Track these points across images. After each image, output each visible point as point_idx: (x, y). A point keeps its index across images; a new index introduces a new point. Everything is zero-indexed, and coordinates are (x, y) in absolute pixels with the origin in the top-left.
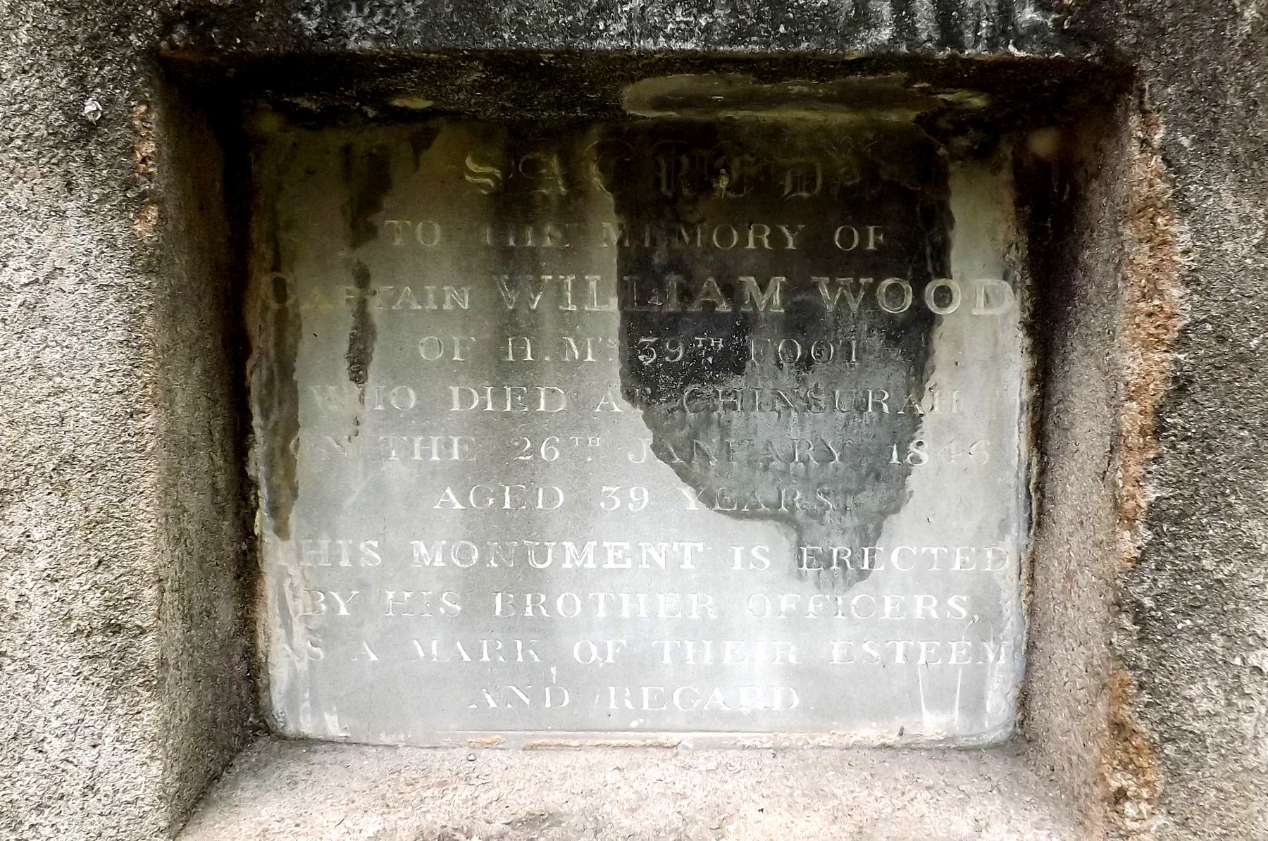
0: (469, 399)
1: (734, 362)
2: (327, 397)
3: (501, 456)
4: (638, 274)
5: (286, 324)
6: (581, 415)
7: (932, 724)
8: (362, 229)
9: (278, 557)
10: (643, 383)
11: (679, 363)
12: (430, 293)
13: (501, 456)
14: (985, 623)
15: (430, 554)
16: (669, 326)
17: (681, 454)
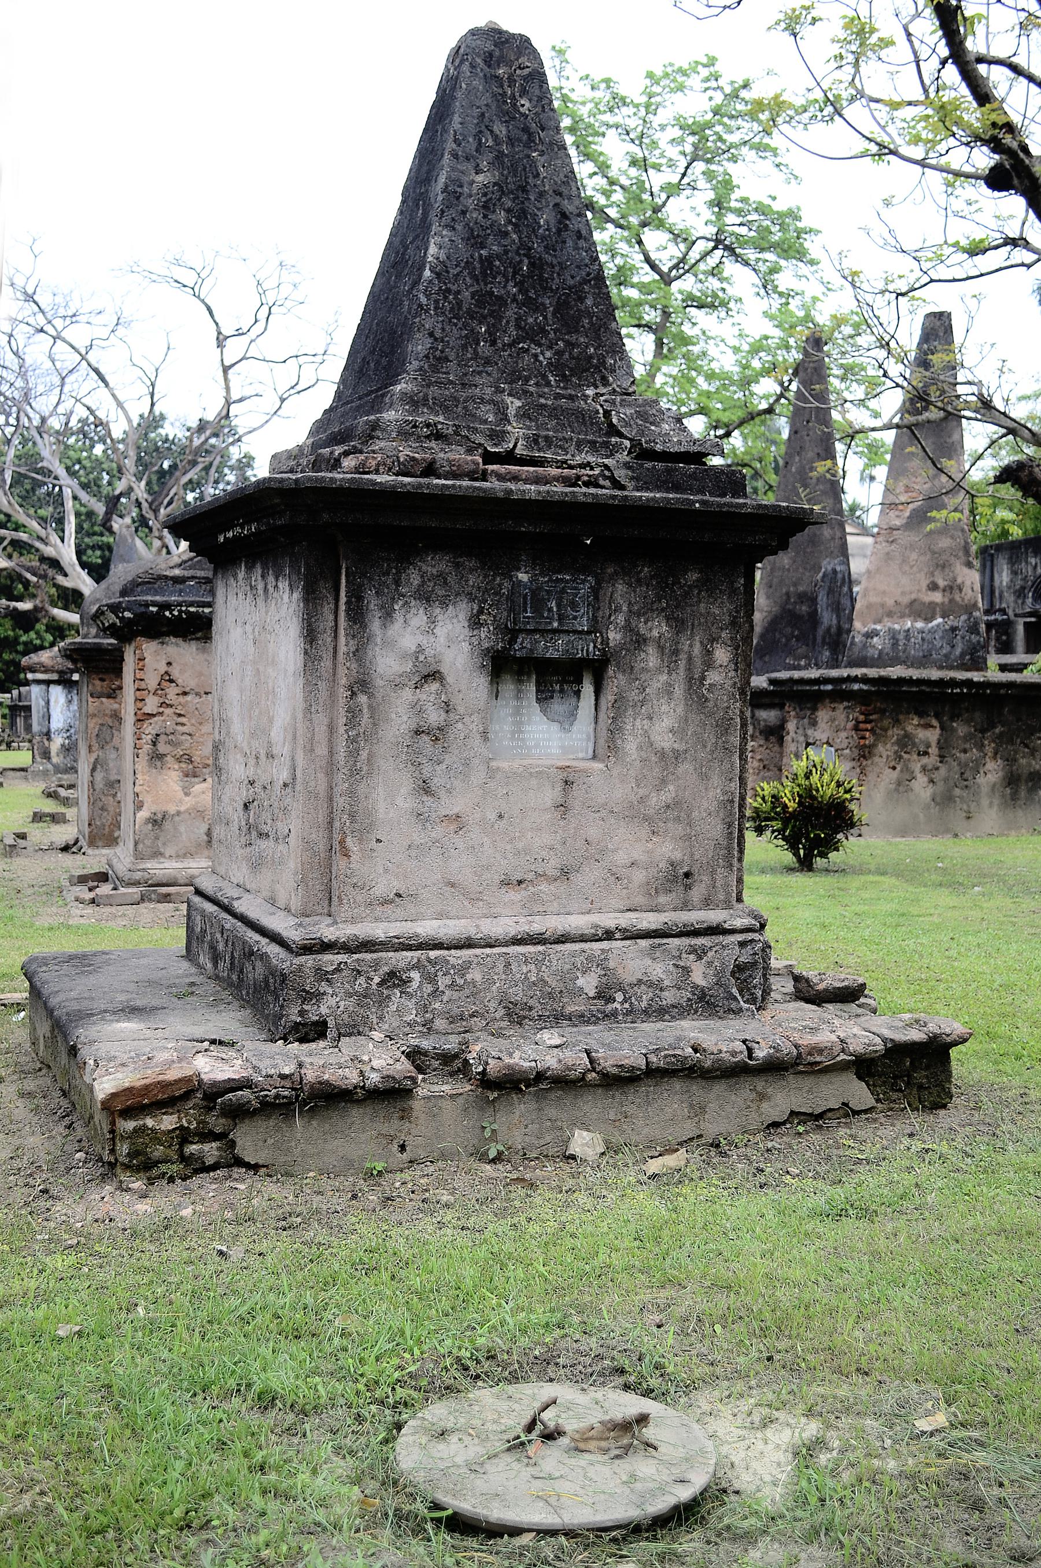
1: (552, 697)
3: (517, 712)
4: (538, 684)
6: (529, 706)
7: (581, 755)
10: (538, 700)
11: (544, 696)
13: (517, 712)
14: (588, 739)
15: (506, 728)
16: (543, 692)
17: (544, 711)
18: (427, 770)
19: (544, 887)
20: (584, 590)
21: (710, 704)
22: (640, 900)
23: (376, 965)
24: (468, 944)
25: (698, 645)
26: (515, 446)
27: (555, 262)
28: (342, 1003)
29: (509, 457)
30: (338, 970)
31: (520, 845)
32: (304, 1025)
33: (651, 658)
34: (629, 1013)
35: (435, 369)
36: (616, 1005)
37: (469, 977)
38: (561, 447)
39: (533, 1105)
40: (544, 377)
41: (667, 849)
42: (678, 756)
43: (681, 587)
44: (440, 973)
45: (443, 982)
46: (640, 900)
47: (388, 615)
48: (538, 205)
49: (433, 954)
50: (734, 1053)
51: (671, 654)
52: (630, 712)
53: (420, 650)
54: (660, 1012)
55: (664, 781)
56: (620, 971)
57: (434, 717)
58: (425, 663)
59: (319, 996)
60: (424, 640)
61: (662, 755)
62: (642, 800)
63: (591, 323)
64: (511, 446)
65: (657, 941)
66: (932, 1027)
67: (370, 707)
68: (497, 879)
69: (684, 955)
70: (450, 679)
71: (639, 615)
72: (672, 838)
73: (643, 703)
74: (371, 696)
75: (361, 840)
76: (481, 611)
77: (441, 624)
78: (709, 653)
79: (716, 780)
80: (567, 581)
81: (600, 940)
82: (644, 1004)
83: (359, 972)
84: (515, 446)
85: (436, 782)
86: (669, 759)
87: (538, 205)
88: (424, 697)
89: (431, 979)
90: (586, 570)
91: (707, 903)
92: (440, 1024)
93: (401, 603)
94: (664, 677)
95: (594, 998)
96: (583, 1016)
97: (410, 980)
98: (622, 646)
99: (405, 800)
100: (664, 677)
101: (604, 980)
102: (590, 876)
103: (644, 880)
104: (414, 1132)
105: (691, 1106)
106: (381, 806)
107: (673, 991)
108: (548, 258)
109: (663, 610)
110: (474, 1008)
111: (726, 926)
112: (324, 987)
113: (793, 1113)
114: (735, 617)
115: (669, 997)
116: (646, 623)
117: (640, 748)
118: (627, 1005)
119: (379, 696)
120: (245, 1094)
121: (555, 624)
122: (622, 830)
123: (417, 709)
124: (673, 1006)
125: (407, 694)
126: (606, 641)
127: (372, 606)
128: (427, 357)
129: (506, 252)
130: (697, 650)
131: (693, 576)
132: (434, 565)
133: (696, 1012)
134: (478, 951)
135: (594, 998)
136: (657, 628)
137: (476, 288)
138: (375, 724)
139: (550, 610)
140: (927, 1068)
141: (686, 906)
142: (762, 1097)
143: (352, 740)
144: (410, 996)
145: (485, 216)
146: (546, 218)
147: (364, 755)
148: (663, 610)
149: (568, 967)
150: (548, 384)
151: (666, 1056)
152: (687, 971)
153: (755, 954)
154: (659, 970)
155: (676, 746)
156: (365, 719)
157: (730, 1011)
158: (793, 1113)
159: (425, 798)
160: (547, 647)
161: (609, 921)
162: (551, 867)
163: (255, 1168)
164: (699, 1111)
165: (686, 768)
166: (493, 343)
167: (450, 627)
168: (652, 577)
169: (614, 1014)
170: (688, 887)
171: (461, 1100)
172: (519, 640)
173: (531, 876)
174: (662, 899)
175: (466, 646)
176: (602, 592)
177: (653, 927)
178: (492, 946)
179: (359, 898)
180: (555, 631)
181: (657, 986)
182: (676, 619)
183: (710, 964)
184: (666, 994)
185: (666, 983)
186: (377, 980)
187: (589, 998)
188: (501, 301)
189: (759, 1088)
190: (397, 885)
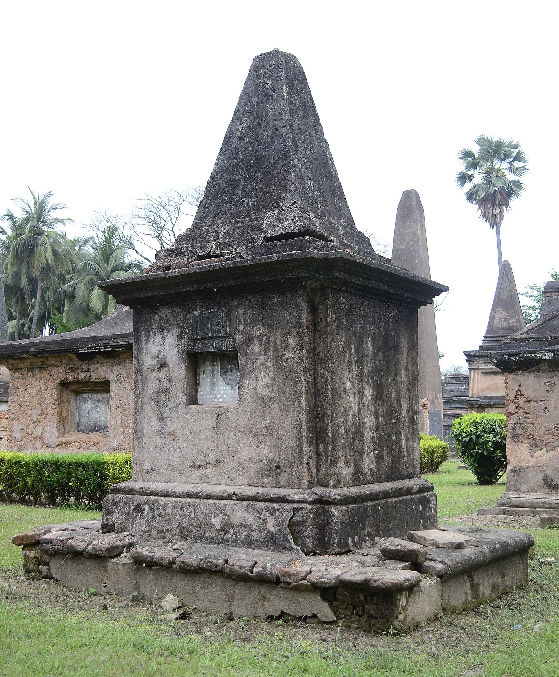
0: (211, 376)
2: (202, 376)
3: (212, 381)
4: (221, 366)
5: (199, 371)
6: (217, 377)
8: (204, 363)
9: (199, 389)
10: (221, 374)
12: (208, 368)
18: (162, 409)
19: (210, 470)
20: (223, 315)
21: (287, 370)
22: (254, 480)
23: (133, 500)
24: (167, 495)
25: (279, 337)
26: (210, 251)
27: (267, 154)
28: (120, 517)
29: (209, 256)
30: (119, 501)
31: (199, 447)
32: (108, 525)
33: (256, 347)
34: (234, 541)
35: (202, 222)
36: (229, 536)
37: (166, 511)
38: (231, 246)
39: (154, 576)
40: (249, 212)
41: (267, 452)
42: (271, 400)
43: (270, 307)
44: (156, 508)
45: (156, 512)
46: (254, 480)
47: (148, 339)
48: (265, 129)
49: (154, 498)
50: (241, 567)
51: (266, 344)
52: (247, 377)
53: (159, 353)
54: (249, 543)
55: (264, 414)
56: (232, 517)
57: (165, 384)
58: (161, 359)
59: (113, 512)
60: (159, 348)
61: (263, 399)
62: (253, 424)
63: (279, 179)
64: (209, 251)
65: (252, 503)
66: (369, 576)
67: (141, 381)
68: (190, 464)
69: (264, 512)
70: (170, 366)
71: (249, 325)
72: (269, 446)
73: (253, 371)
74: (142, 376)
75: (139, 442)
76: (182, 332)
77: (167, 340)
78: (285, 341)
79: (291, 413)
80: (215, 312)
81: (225, 499)
82: (242, 537)
83: (126, 503)
84: (210, 251)
85: (166, 415)
86: (266, 401)
87: (265, 129)
88: (161, 375)
89: (152, 510)
90: (224, 305)
91: (289, 485)
92: (154, 533)
93: (152, 332)
94: (263, 357)
95: (219, 530)
96: (213, 539)
97: (143, 510)
98: (242, 342)
99: (154, 425)
100: (263, 357)
101: (224, 521)
102: (230, 465)
103: (255, 469)
104: (109, 578)
105: (227, 595)
106: (146, 427)
107: (257, 532)
108: (264, 153)
109: (261, 320)
110: (168, 527)
111: (289, 498)
112: (115, 509)
113: (283, 613)
114: (298, 319)
115: (255, 535)
116: (253, 328)
117: (252, 396)
118: (234, 537)
119: (145, 375)
120: (49, 546)
121: (210, 334)
122: (244, 441)
123: (158, 380)
124: (257, 541)
125: (155, 374)
126: (234, 340)
127: (142, 335)
128: (200, 217)
129: (245, 157)
130: (279, 340)
131: (275, 300)
132: (164, 312)
133: (268, 546)
134: (171, 499)
135: (219, 530)
136: (259, 331)
137: (229, 178)
138: (143, 389)
139: (208, 328)
140: (377, 603)
141: (277, 485)
142: (265, 598)
143: (136, 396)
144: (144, 517)
145: (240, 143)
146: (267, 134)
147: (140, 402)
148: (261, 320)
149: (208, 511)
150: (250, 215)
151: (208, 562)
152: (265, 521)
153: (303, 516)
154: (251, 519)
155: (270, 394)
156: (140, 387)
157: (285, 548)
158: (283, 613)
159: (162, 423)
160: (209, 346)
161: (231, 489)
162: (212, 459)
163: (57, 580)
164: (230, 599)
165: (275, 406)
166: (230, 202)
167: (170, 341)
168: (255, 304)
169: (227, 540)
170: (278, 475)
171: (126, 567)
172: (197, 344)
173: (203, 464)
174: (265, 480)
175: (176, 349)
176: (232, 315)
177: (250, 494)
178: (179, 497)
179: (138, 470)
180: (212, 338)
181: (249, 528)
182: (268, 325)
183: (277, 519)
184: (254, 533)
185: (254, 527)
186: (132, 508)
187: (217, 530)
188: (239, 180)
189: (263, 592)
190: (152, 465)
